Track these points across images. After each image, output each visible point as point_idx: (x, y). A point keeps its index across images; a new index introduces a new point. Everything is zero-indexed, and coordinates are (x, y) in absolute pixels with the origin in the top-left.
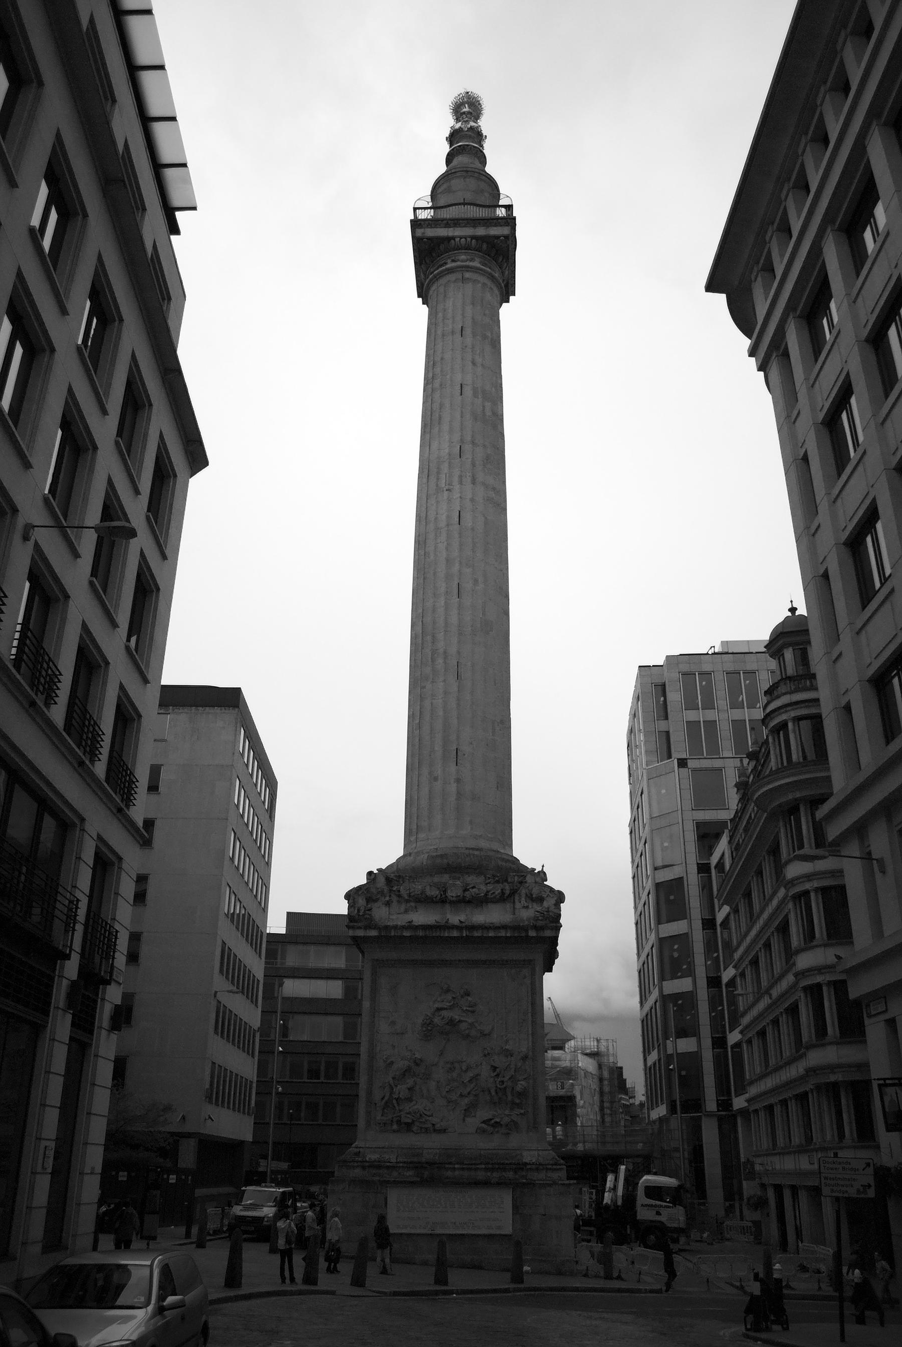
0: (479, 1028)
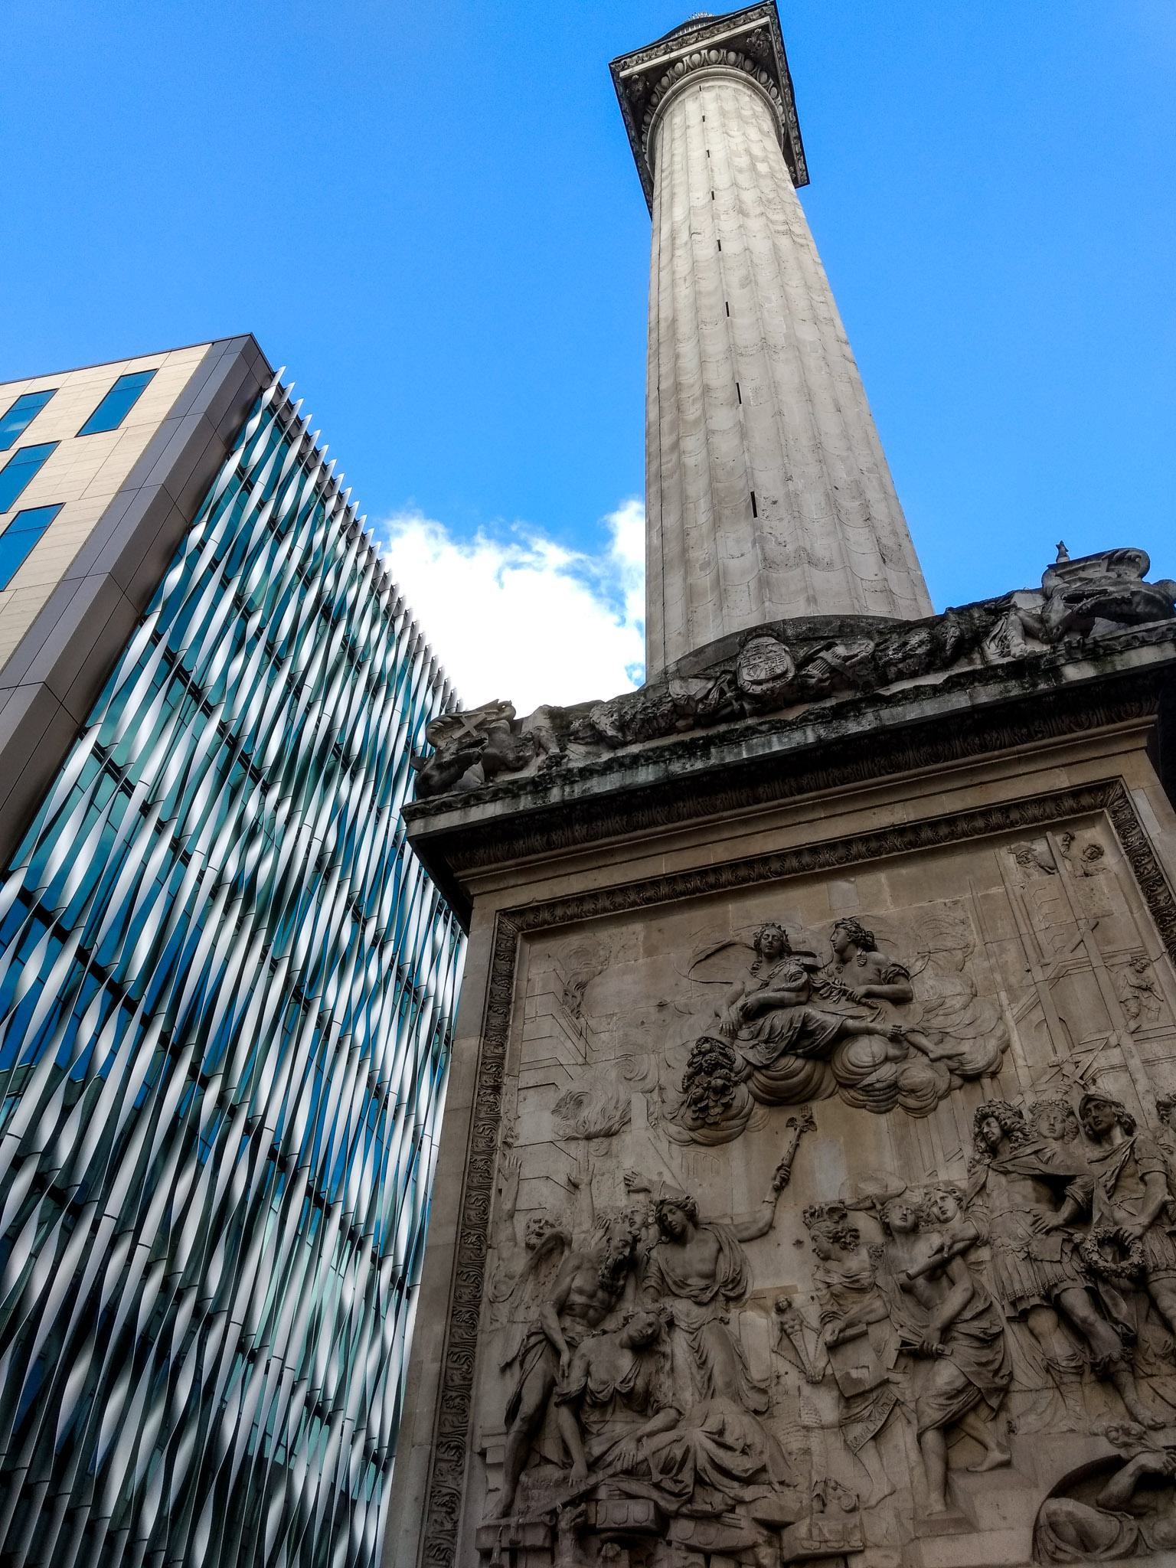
0: (937, 1051)
